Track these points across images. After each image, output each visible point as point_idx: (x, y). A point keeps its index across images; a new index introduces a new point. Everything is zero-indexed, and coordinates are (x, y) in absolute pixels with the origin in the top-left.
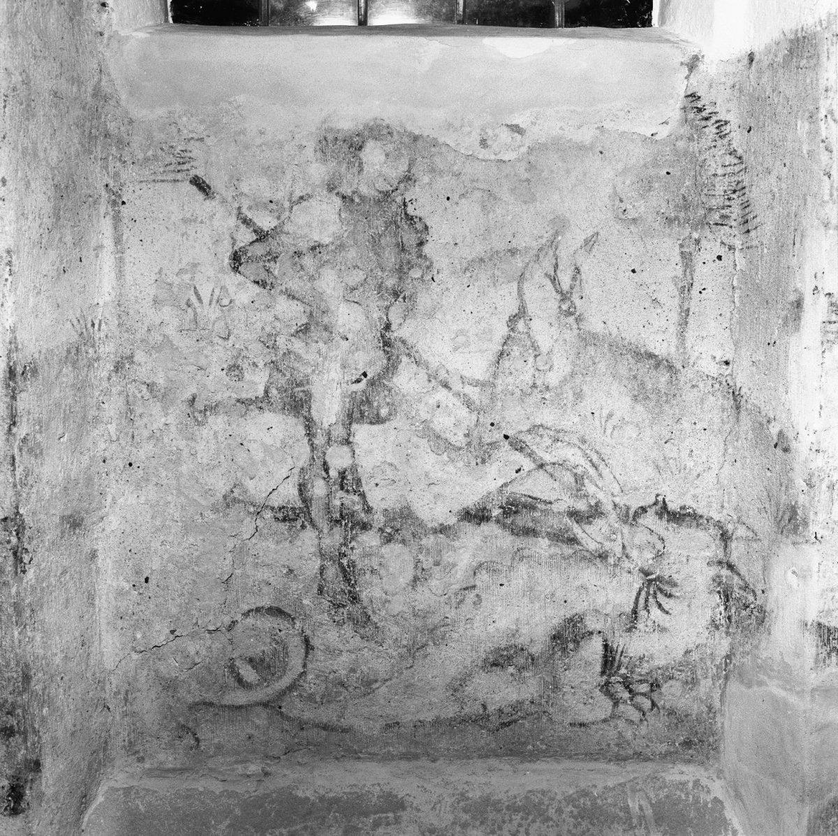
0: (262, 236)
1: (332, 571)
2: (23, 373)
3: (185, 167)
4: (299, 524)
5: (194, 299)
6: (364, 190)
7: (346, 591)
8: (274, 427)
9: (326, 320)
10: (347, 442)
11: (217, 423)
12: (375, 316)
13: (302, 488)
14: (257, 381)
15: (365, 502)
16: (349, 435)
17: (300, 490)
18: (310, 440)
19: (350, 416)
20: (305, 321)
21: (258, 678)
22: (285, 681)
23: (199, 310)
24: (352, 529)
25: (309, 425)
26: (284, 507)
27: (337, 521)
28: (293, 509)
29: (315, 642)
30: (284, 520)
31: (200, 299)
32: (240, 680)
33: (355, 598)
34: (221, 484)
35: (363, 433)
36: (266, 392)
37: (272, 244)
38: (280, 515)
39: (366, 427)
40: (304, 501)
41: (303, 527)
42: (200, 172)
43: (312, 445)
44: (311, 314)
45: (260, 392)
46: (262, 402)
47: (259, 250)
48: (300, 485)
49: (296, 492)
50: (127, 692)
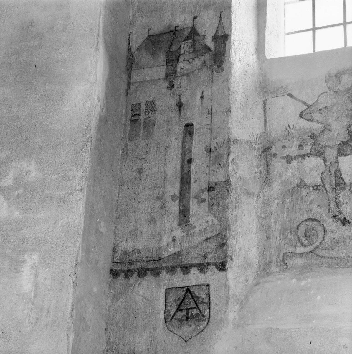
0: (309, 107)
1: (333, 205)
2: (233, 141)
3: (286, 91)
4: (321, 190)
5: (288, 128)
6: (341, 88)
7: (338, 211)
8: (314, 162)
9: (330, 128)
10: (337, 162)
11: (294, 163)
12: (345, 124)
13: (322, 179)
14: (307, 149)
15: (343, 181)
16: (337, 160)
17: (322, 180)
18: (325, 164)
19: (338, 155)
20: (323, 129)
21: (308, 243)
22: (317, 244)
23: (289, 131)
24: (339, 190)
25: (325, 160)
26: (316, 186)
27: (334, 188)
28: (319, 186)
29: (328, 229)
30: (316, 189)
31: (290, 128)
32: (302, 244)
33: (341, 213)
34: (296, 181)
35: (341, 159)
36: (311, 151)
37: (313, 108)
38: (315, 188)
39: (343, 157)
40: (323, 183)
41: (323, 191)
42: (290, 92)
43: (325, 165)
44: (325, 127)
45: (309, 151)
46: (309, 155)
47: (308, 111)
48: (321, 178)
49: (320, 180)
50: (264, 251)
